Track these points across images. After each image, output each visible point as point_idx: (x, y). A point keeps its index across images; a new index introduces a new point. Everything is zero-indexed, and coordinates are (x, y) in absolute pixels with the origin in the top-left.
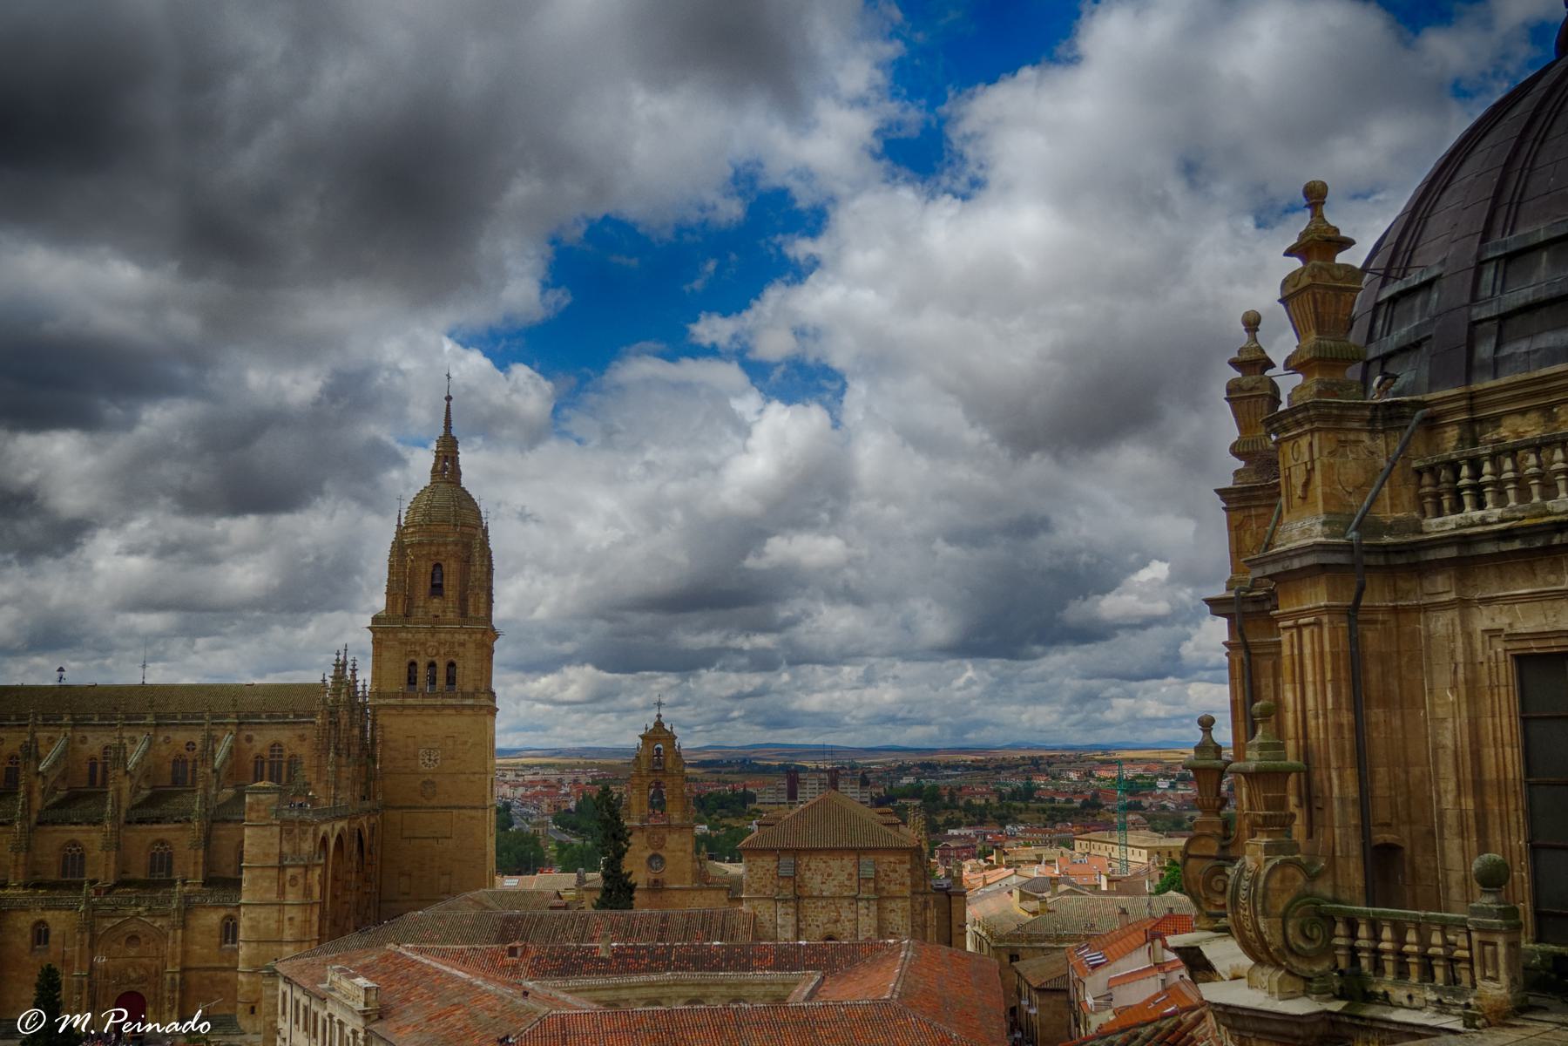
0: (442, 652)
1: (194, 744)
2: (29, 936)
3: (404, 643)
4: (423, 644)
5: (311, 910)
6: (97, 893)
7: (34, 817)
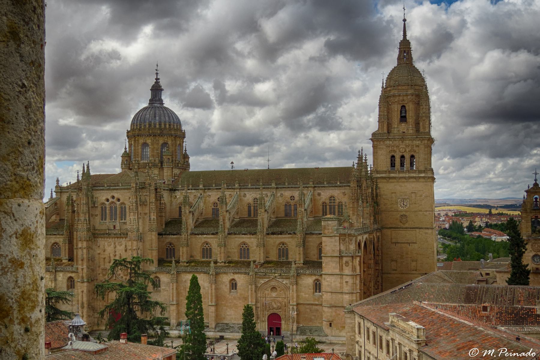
0: (408, 150)
1: (294, 197)
2: (228, 286)
4: (398, 146)
5: (356, 278)
6: (257, 267)
7: (226, 231)
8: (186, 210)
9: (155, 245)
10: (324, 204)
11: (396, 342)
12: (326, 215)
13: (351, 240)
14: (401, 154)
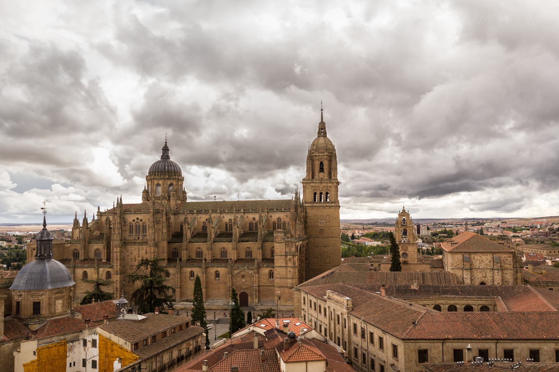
2: (214, 275)
3: (312, 187)
7: (212, 240)
8: (186, 227)
9: (166, 249)
10: (274, 223)
11: (332, 309)
12: (275, 230)
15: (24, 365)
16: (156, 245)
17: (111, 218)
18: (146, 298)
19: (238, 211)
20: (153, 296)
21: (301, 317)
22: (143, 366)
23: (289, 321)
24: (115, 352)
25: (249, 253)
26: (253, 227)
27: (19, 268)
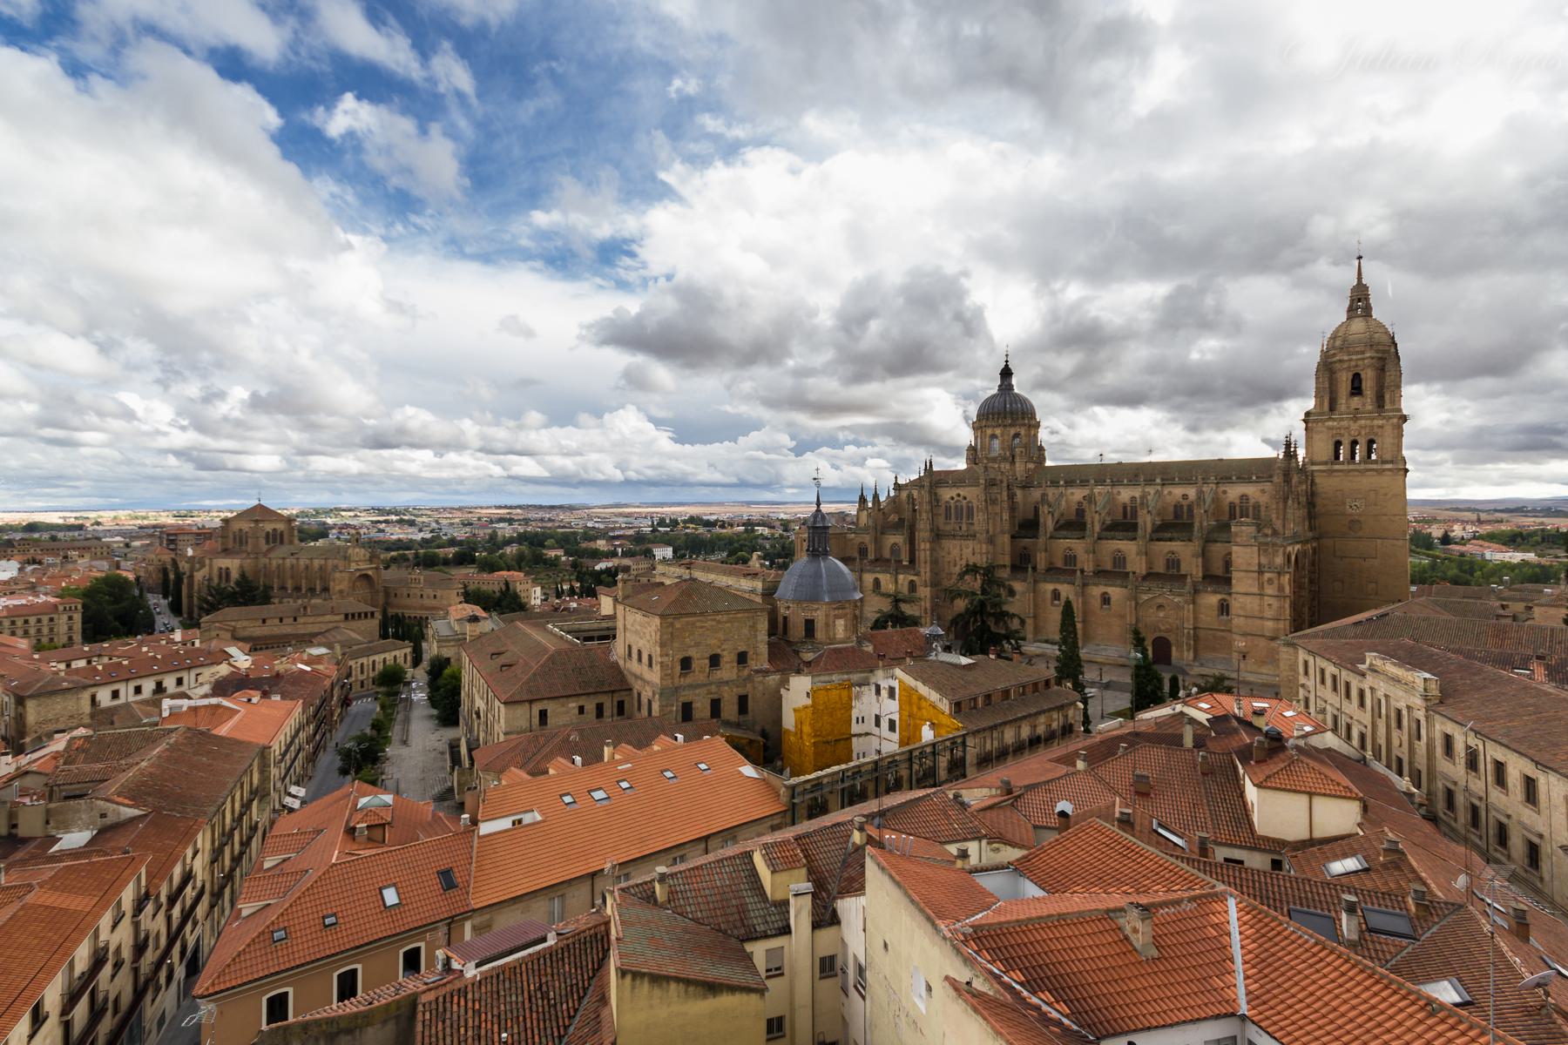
0: (1363, 433)
2: (1099, 601)
3: (1331, 428)
7: (1096, 535)
8: (1044, 509)
9: (1008, 548)
10: (1232, 506)
13: (1277, 551)
14: (1352, 438)
15: (795, 710)
16: (991, 541)
17: (915, 493)
18: (974, 630)
19: (1150, 481)
20: (984, 629)
21: (1298, 701)
22: (970, 742)
23: (1266, 705)
24: (924, 712)
25: (1173, 563)
26: (1183, 512)
27: (785, 567)
